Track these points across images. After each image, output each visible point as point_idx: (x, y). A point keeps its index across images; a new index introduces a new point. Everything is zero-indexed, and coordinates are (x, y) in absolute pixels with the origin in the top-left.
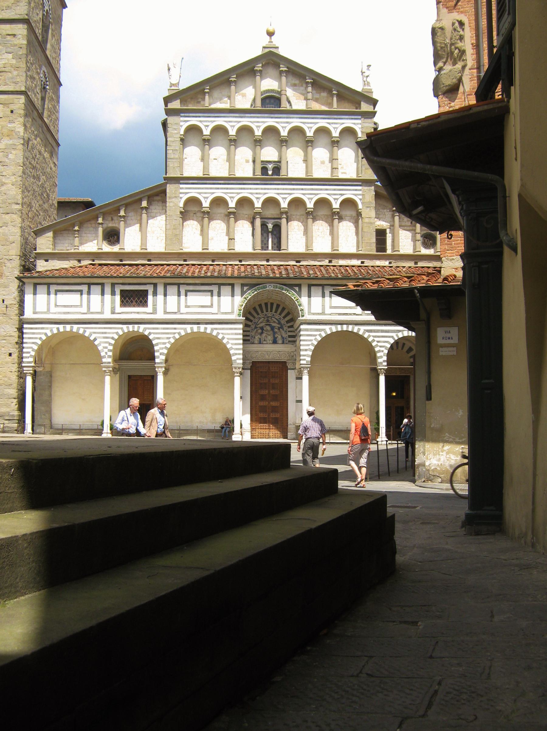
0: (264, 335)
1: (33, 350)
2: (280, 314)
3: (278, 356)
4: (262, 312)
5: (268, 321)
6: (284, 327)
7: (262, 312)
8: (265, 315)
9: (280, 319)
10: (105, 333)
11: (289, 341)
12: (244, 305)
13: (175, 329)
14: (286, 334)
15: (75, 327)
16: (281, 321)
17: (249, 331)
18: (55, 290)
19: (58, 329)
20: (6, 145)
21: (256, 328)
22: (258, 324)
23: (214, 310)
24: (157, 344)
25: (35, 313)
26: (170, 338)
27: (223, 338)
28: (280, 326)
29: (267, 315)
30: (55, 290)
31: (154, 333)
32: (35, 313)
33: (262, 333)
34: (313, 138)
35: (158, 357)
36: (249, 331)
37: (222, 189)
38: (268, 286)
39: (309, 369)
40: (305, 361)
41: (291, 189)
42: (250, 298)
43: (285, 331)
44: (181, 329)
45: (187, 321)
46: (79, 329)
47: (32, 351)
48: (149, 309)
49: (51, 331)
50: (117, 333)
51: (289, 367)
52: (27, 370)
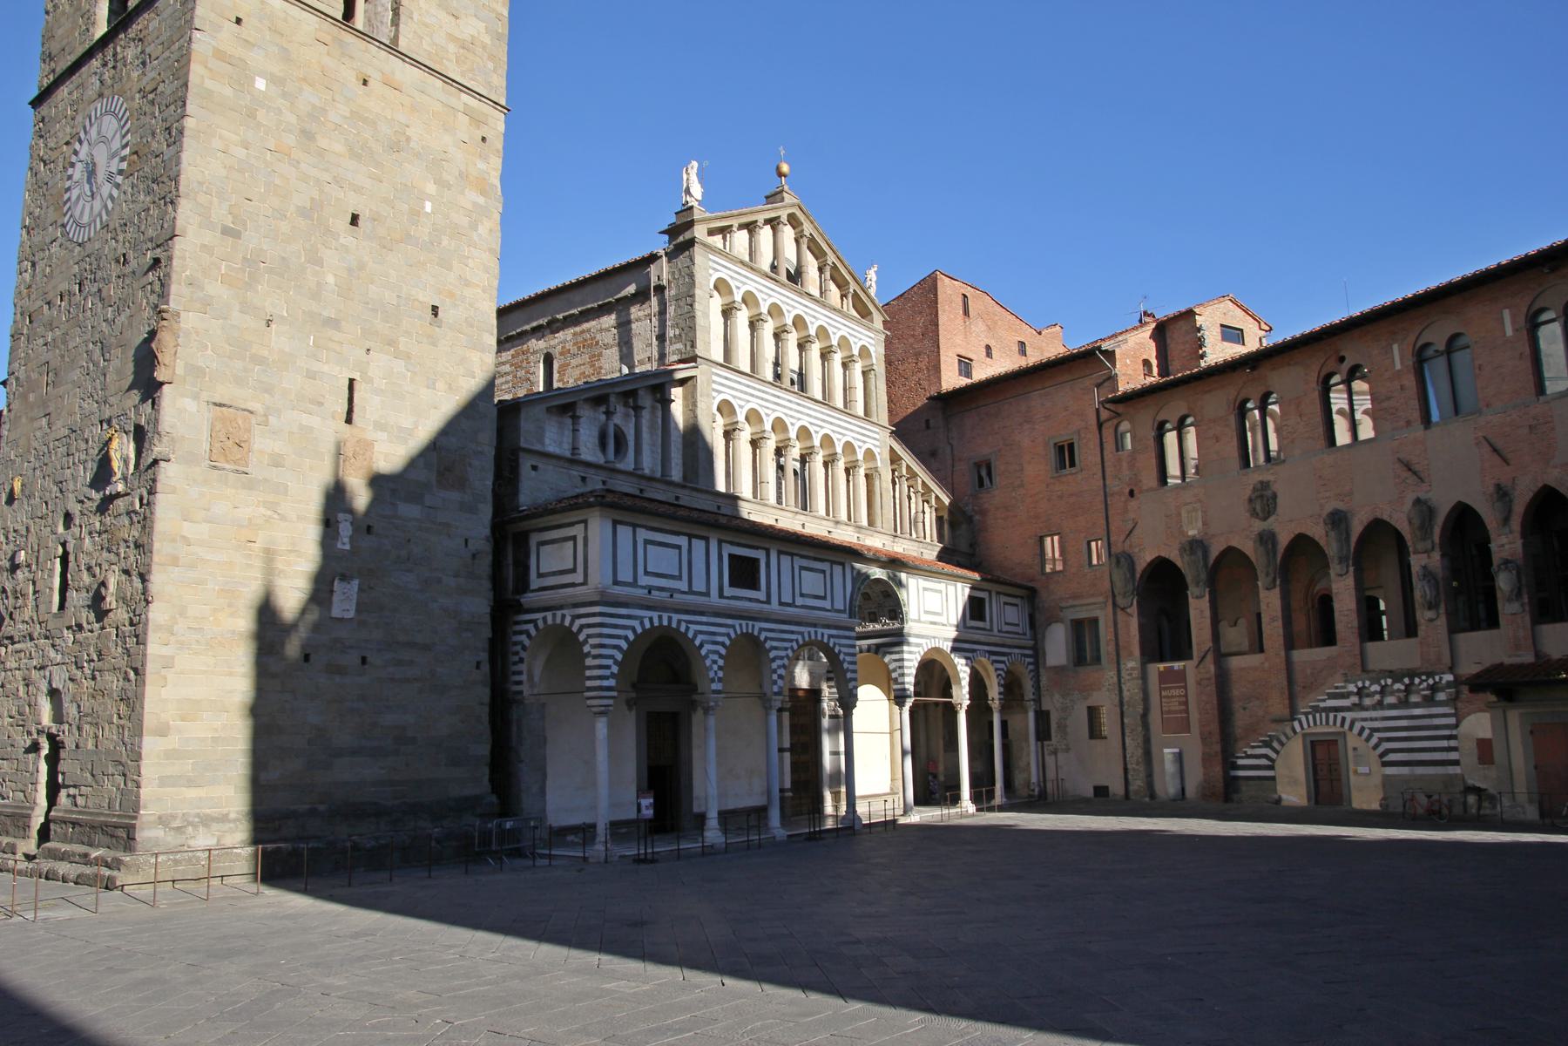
1: (616, 662)
10: (714, 634)
13: (792, 632)
15: (675, 617)
18: (645, 540)
19: (651, 619)
20: (475, 204)
23: (827, 604)
24: (774, 660)
25: (616, 582)
26: (786, 649)
27: (840, 651)
30: (645, 540)
31: (773, 639)
32: (616, 582)
35: (775, 683)
37: (757, 397)
44: (798, 633)
45: (805, 621)
46: (679, 622)
47: (614, 663)
48: (761, 595)
49: (642, 623)
50: (728, 635)
52: (605, 706)
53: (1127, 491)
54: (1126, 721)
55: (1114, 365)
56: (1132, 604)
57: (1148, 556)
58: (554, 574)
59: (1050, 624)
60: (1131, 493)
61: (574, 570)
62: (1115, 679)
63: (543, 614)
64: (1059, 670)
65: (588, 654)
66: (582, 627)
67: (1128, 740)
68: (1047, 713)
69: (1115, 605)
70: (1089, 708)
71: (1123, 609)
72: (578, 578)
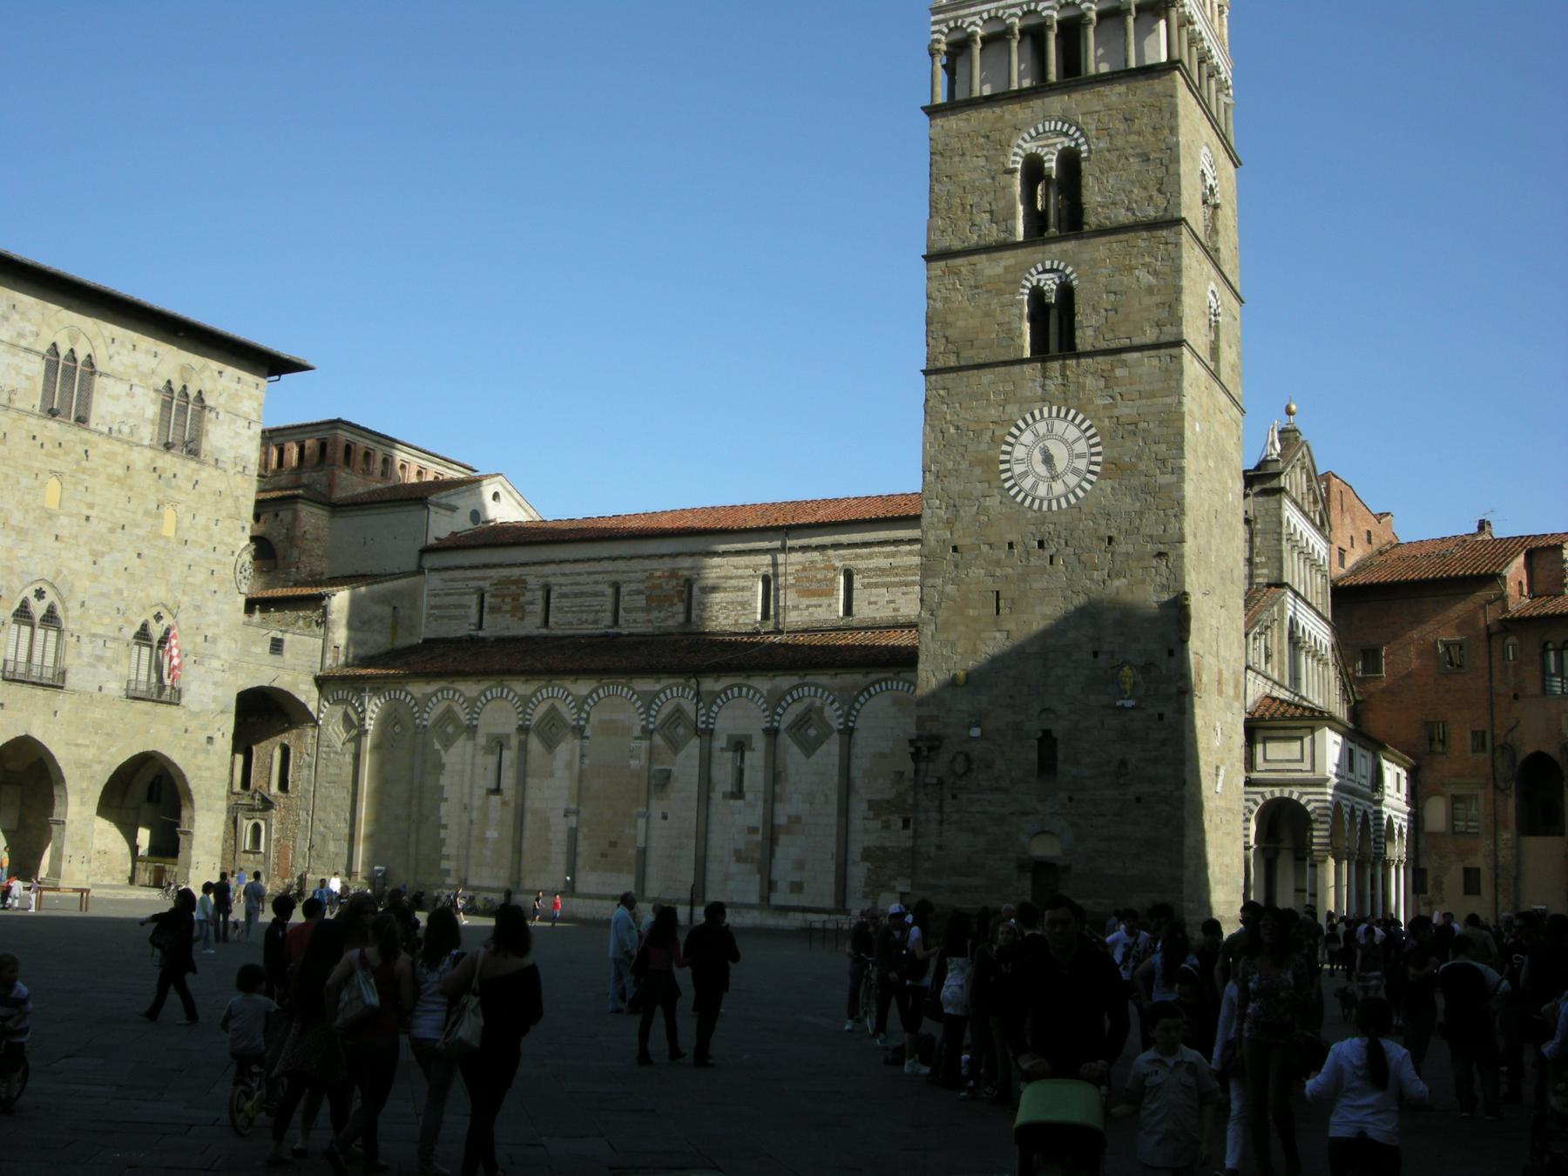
53: (1512, 694)
54: (1499, 881)
55: (1505, 587)
56: (1510, 787)
57: (1529, 749)
58: (1281, 761)
59: (1429, 797)
60: (1516, 697)
61: (1302, 760)
62: (1492, 847)
63: (1271, 789)
64: (1434, 835)
65: (1316, 821)
66: (1309, 801)
67: (1500, 897)
68: (1424, 871)
69: (1496, 787)
70: (1467, 871)
71: (1502, 790)
72: (1306, 765)
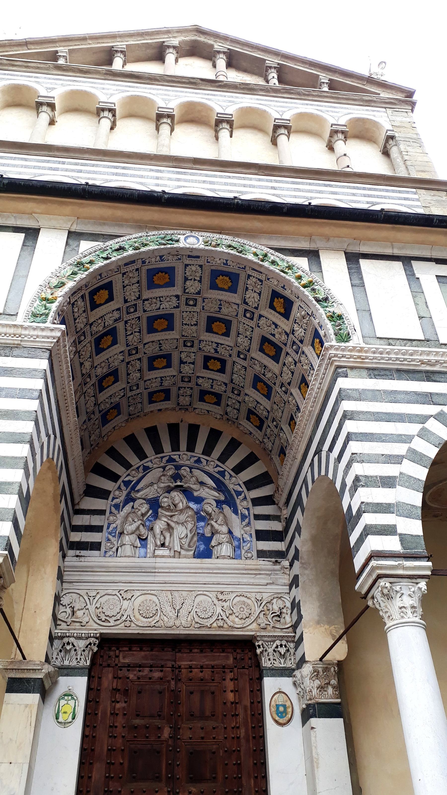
0: (159, 525)
2: (223, 458)
3: (219, 610)
4: (158, 449)
5: (176, 477)
6: (238, 501)
7: (158, 449)
8: (168, 461)
9: (222, 474)
11: (261, 554)
12: (70, 284)
14: (249, 524)
16: (227, 482)
17: (102, 512)
21: (129, 499)
22: (138, 491)
28: (222, 498)
29: (174, 460)
33: (156, 516)
34: (289, 122)
36: (102, 512)
38: (182, 238)
39: (423, 584)
40: (397, 538)
41: (245, 186)
42: (101, 268)
43: (243, 517)
51: (266, 663)
